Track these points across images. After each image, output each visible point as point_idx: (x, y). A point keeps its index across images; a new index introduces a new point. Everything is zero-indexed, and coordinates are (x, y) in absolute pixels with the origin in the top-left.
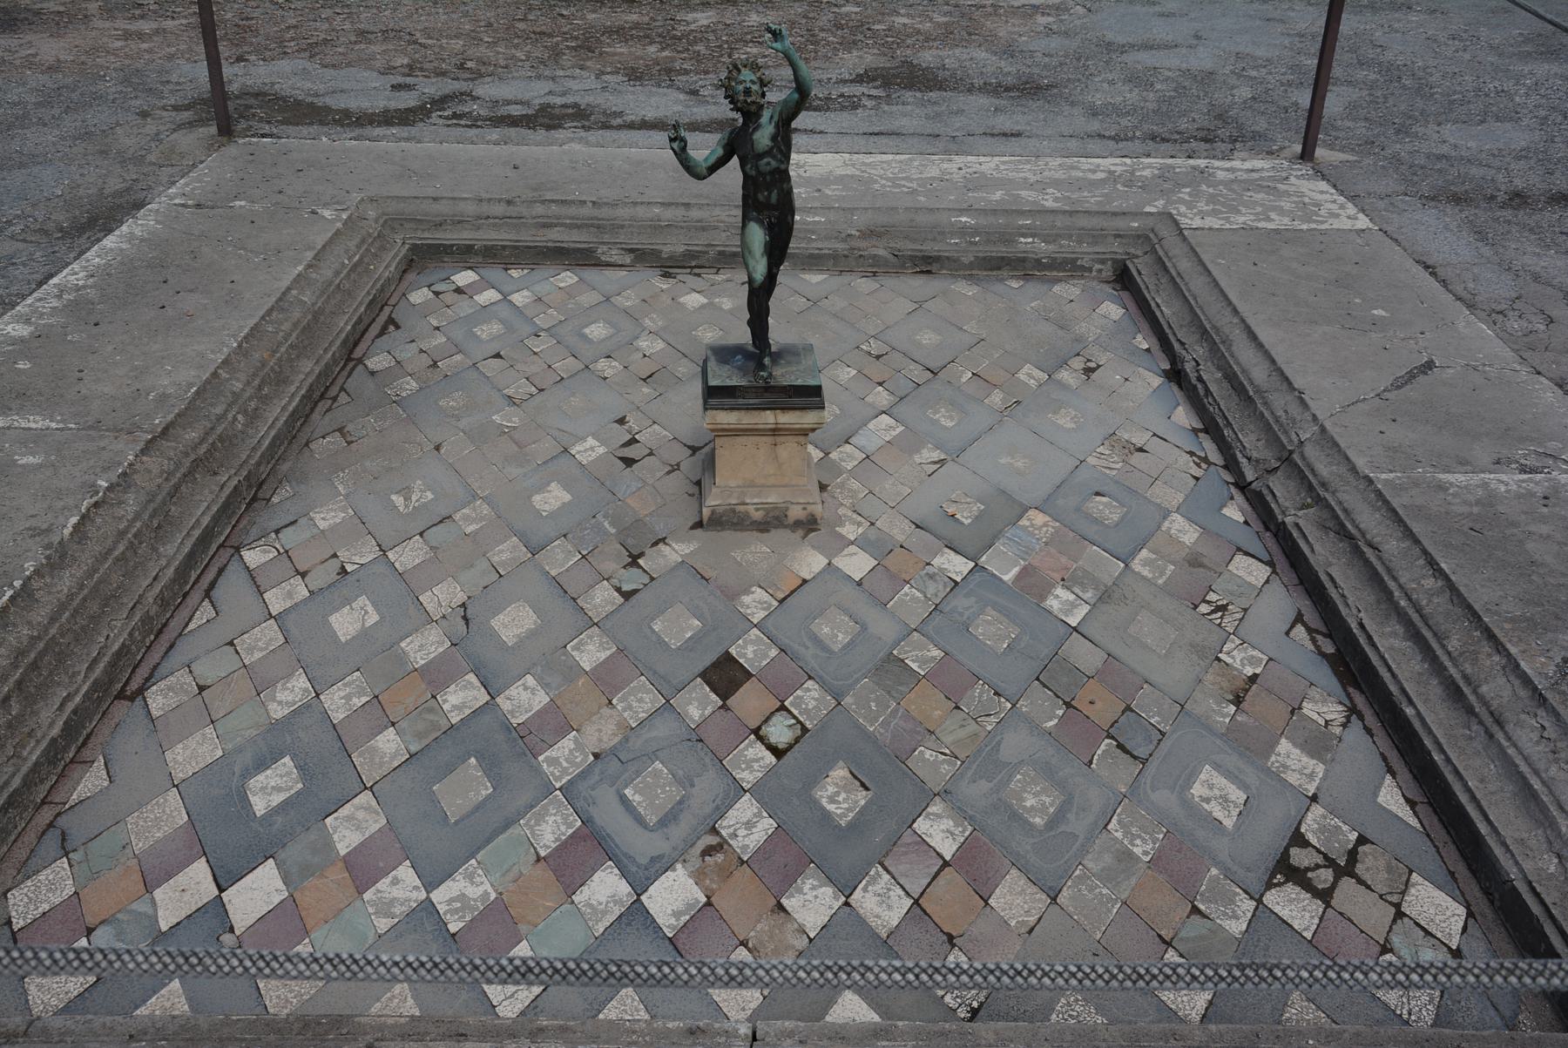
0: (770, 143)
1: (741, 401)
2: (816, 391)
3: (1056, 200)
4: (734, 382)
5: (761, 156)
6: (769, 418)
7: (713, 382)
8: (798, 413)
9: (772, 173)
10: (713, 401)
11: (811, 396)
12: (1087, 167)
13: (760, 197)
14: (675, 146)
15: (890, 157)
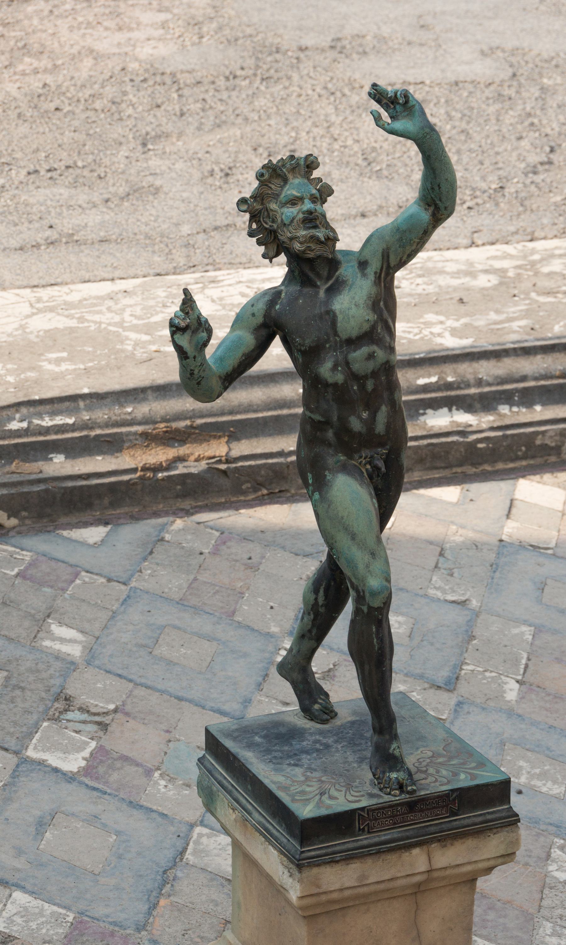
0: (372, 317)
1: (364, 839)
2: (501, 790)
3: (454, 332)
4: (341, 802)
5: (353, 342)
6: (417, 861)
7: (306, 811)
8: (470, 842)
9: (374, 374)
10: (312, 850)
11: (483, 806)
12: (451, 267)
13: (356, 424)
14: (184, 341)
15: (106, 288)
